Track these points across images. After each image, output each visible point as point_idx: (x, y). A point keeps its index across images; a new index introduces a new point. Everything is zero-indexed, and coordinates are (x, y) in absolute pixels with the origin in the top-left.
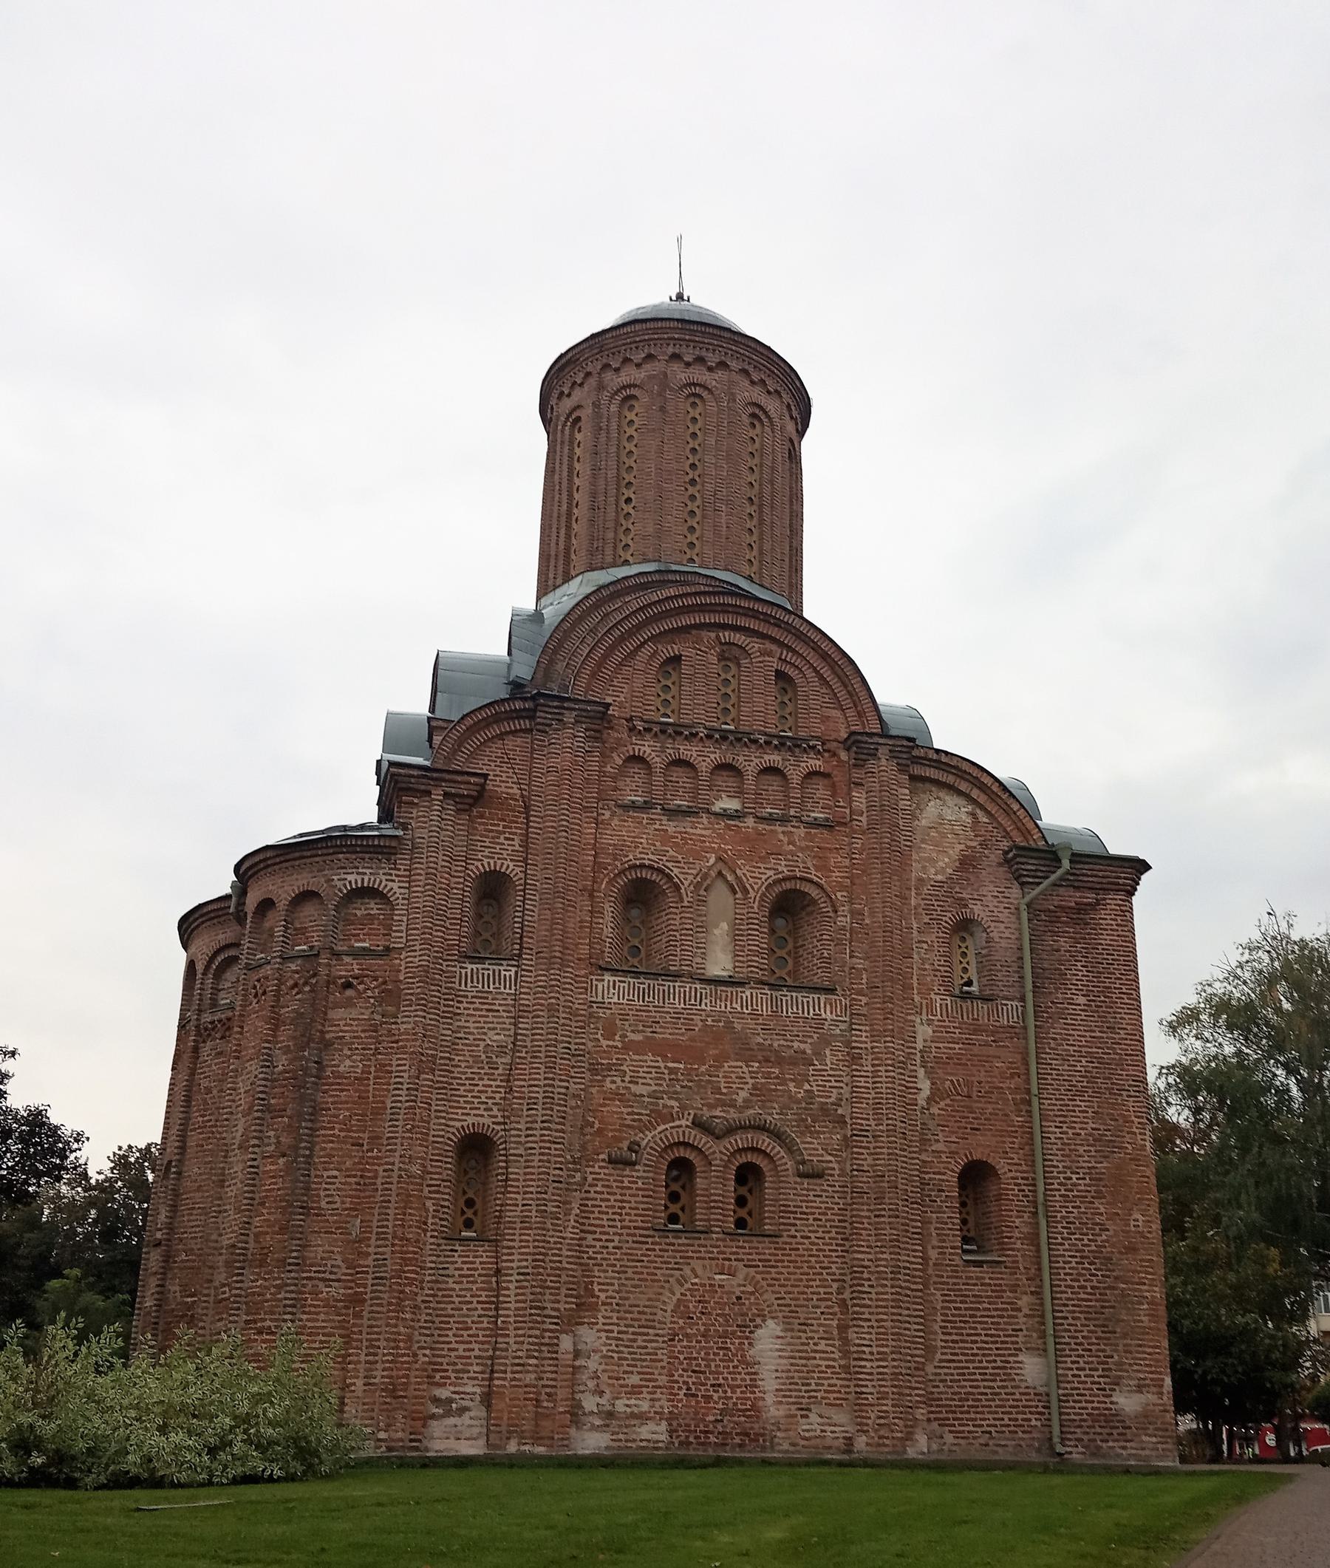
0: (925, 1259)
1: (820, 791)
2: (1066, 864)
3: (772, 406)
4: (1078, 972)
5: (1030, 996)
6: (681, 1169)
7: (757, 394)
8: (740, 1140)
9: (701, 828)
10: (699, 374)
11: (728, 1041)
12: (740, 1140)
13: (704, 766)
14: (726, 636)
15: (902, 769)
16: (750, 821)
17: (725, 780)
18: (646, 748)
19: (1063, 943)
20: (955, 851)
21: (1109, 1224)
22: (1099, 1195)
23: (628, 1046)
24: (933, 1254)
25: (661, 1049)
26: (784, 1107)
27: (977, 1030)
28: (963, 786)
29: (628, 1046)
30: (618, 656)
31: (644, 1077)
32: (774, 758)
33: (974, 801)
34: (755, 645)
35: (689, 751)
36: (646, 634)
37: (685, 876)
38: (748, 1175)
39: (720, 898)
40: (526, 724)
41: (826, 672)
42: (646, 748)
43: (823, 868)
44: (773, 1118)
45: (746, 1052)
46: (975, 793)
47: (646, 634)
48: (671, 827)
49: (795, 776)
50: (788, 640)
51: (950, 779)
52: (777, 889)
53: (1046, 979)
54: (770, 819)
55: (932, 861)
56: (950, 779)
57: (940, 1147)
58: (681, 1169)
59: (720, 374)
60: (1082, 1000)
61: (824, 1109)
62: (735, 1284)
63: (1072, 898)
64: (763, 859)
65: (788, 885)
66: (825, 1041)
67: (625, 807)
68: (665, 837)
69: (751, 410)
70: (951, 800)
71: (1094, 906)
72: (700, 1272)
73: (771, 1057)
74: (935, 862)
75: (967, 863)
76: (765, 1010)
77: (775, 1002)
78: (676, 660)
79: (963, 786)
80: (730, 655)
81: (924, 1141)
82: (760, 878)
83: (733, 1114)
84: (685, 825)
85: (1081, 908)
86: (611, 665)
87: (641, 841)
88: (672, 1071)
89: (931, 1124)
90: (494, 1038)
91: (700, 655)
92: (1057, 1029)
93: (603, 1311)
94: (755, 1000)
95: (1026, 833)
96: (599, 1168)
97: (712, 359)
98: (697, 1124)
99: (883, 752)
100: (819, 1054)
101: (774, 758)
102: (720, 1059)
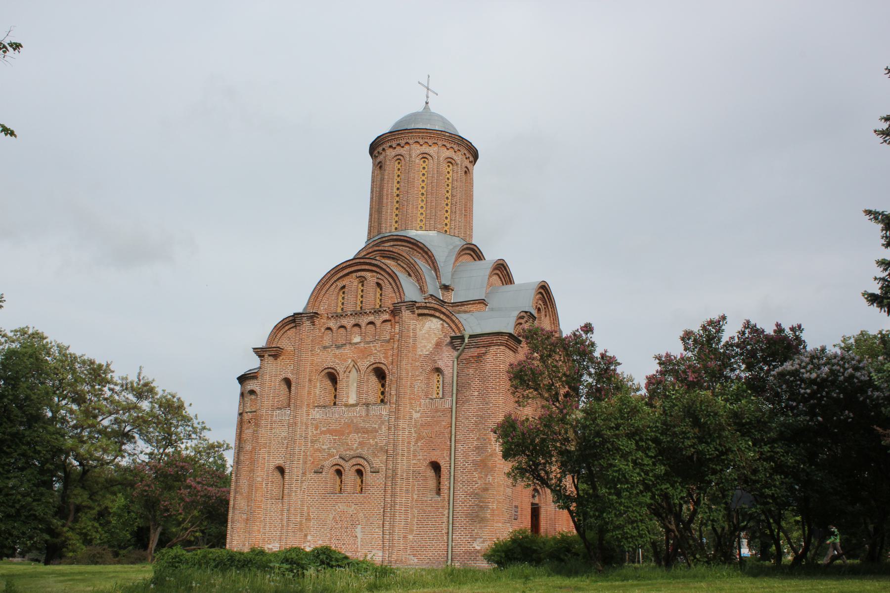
0: (413, 499)
1: (388, 326)
2: (466, 340)
3: (433, 150)
4: (476, 383)
5: (454, 395)
6: (339, 473)
7: (425, 149)
8: (354, 461)
9: (347, 350)
10: (399, 150)
11: (353, 427)
12: (354, 461)
13: (349, 327)
14: (359, 274)
15: (413, 312)
16: (362, 345)
17: (356, 329)
18: (332, 324)
19: (471, 371)
20: (434, 340)
21: (479, 482)
22: (476, 470)
23: (322, 433)
24: (415, 497)
25: (330, 432)
26: (369, 448)
27: (436, 412)
28: (437, 314)
29: (322, 433)
30: (324, 291)
31: (326, 442)
32: (371, 318)
33: (442, 319)
34: (368, 275)
35: (344, 322)
36: (333, 280)
37: (340, 369)
38: (360, 473)
39: (354, 374)
40: (293, 325)
41: (390, 280)
42: (332, 324)
43: (386, 357)
44: (364, 453)
45: (358, 430)
46: (442, 316)
47: (333, 280)
48: (337, 352)
49: (378, 323)
50: (378, 270)
51: (432, 312)
52: (371, 368)
53: (462, 387)
54: (368, 343)
55: (425, 346)
56: (432, 312)
57: (420, 457)
58: (339, 473)
59: (407, 147)
60: (476, 393)
61: (381, 448)
62: (351, 510)
63: (474, 352)
64: (366, 358)
65: (374, 366)
66: (382, 423)
67: (325, 348)
68: (335, 356)
69: (421, 156)
70: (435, 320)
71: (484, 354)
72: (341, 507)
73: (366, 431)
74: (425, 346)
75: (438, 345)
76: (364, 414)
77: (368, 410)
78: (344, 287)
79: (437, 314)
80: (362, 280)
81: (415, 456)
82: (364, 364)
83: (352, 453)
84: (341, 351)
85: (479, 356)
86: (321, 295)
87: (328, 359)
88: (335, 439)
89: (418, 449)
90: (284, 434)
91: (352, 282)
92: (466, 406)
93: (312, 521)
94: (361, 410)
95: (459, 329)
96: (310, 475)
97: (403, 142)
98: (341, 458)
99: (403, 308)
100: (380, 428)
101: (371, 318)
102: (349, 434)
